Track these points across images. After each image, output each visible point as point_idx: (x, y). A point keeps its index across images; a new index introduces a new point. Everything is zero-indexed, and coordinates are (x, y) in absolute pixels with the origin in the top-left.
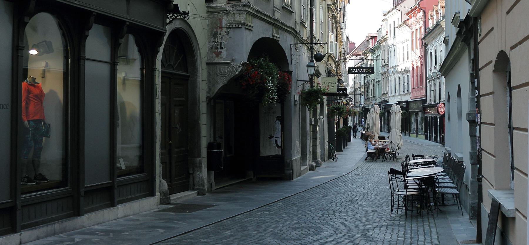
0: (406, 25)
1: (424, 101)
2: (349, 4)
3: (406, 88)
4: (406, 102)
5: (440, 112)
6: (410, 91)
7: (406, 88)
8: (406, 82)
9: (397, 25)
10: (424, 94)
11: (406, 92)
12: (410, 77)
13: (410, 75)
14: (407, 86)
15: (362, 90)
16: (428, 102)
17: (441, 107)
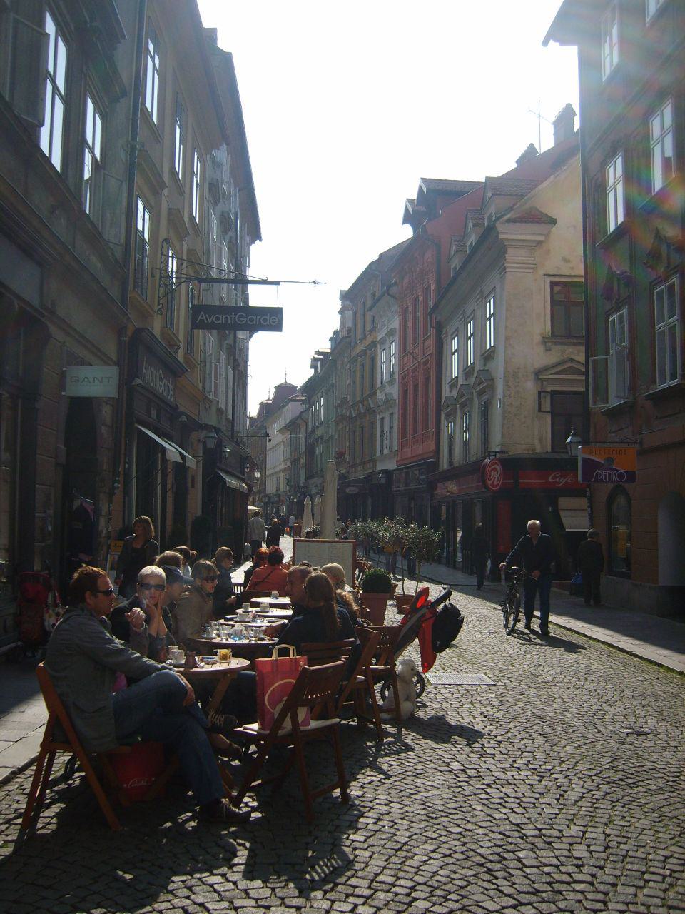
0: (391, 296)
1: (435, 465)
2: (261, 240)
3: (387, 442)
4: (386, 471)
5: (489, 480)
6: (396, 447)
7: (387, 442)
8: (387, 429)
9: (369, 303)
10: (433, 447)
11: (386, 451)
12: (396, 416)
13: (397, 410)
14: (388, 438)
15: (302, 461)
16: (444, 464)
17: (495, 470)
